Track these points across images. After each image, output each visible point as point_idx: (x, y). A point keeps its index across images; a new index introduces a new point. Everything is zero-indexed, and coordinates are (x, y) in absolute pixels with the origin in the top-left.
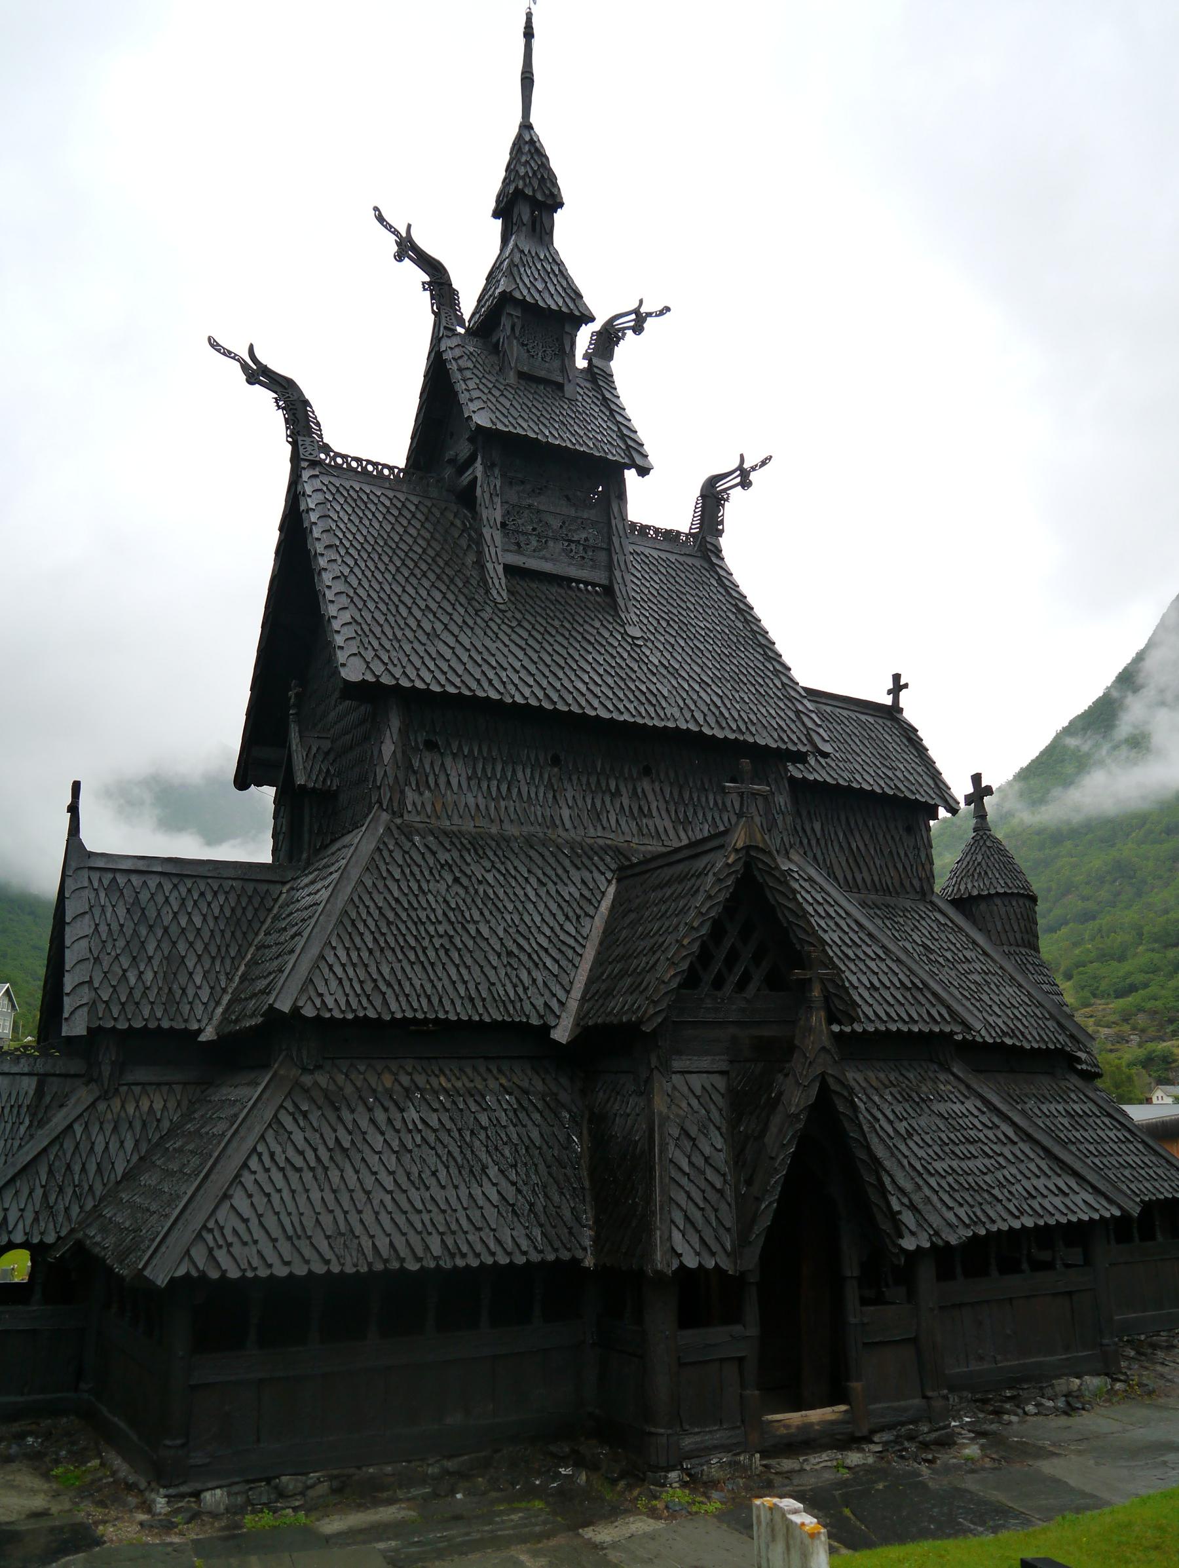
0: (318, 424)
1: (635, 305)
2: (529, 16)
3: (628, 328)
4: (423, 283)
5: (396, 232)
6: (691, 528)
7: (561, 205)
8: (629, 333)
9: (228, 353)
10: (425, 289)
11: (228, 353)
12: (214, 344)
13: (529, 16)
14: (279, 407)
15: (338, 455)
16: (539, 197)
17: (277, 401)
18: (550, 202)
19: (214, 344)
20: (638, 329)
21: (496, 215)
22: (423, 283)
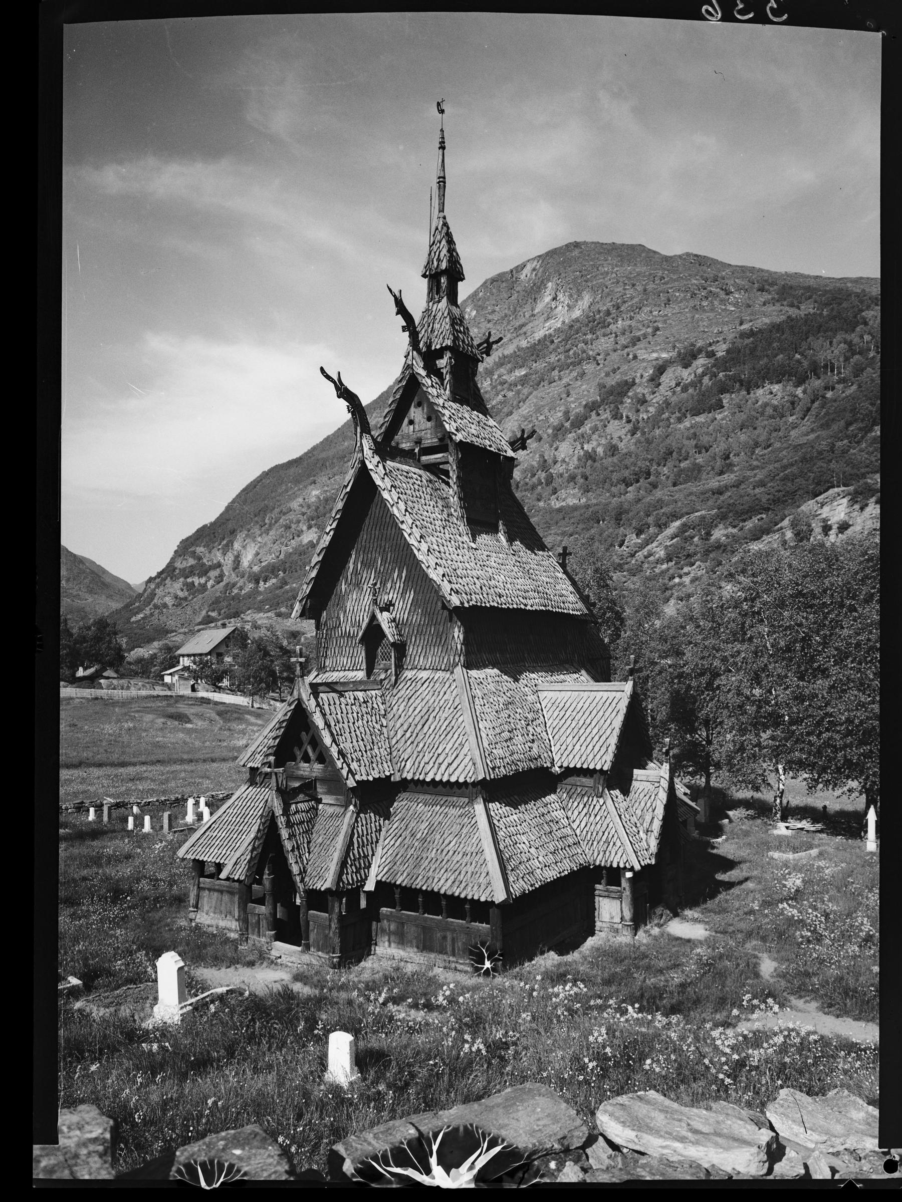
2: (442, 130)
4: (403, 327)
5: (395, 296)
7: (462, 279)
9: (328, 377)
10: (404, 331)
11: (328, 377)
13: (442, 130)
14: (349, 411)
21: (424, 276)
22: (403, 327)
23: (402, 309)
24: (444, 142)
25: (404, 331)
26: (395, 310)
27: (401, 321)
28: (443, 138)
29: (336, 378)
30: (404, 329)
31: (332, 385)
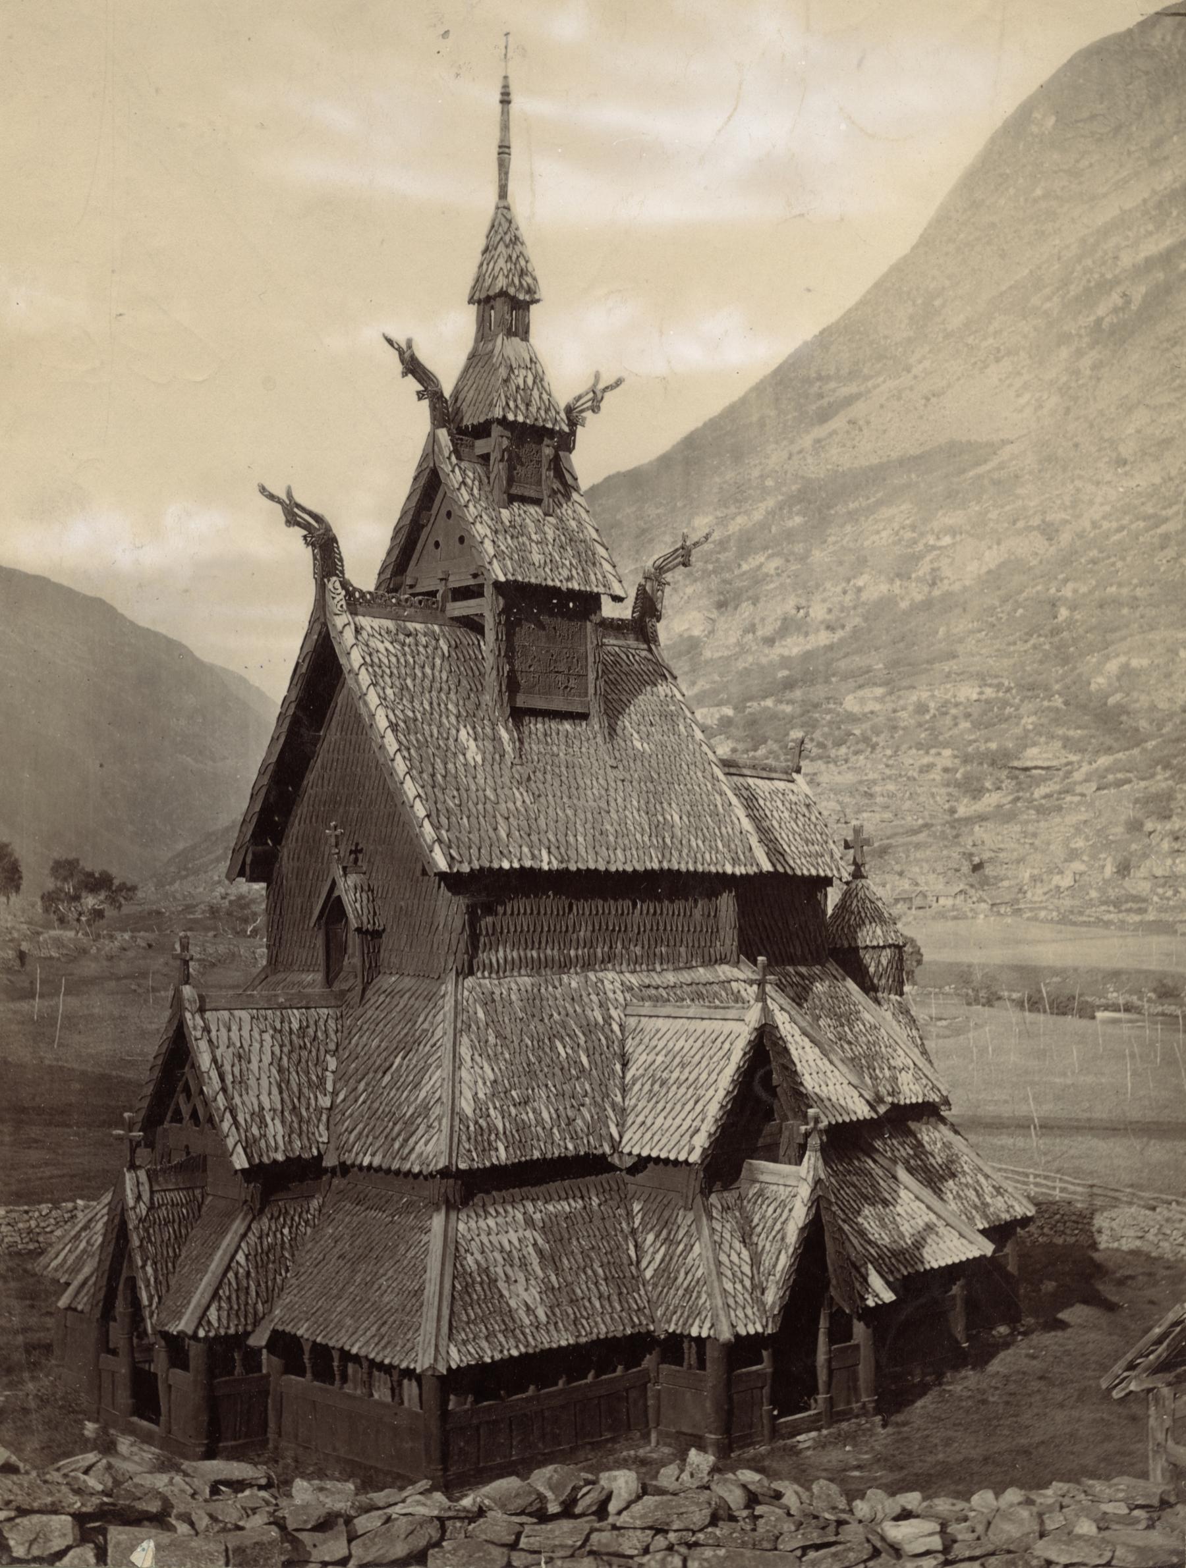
0: (341, 560)
1: (591, 382)
2: (506, 77)
3: (588, 409)
4: (418, 393)
6: (633, 612)
8: (588, 414)
9: (272, 497)
10: (420, 399)
11: (272, 497)
12: (263, 490)
13: (506, 77)
15: (355, 589)
16: (521, 297)
17: (305, 537)
18: (528, 298)
19: (263, 490)
20: (595, 409)
22: (418, 393)
23: (413, 366)
24: (508, 94)
25: (420, 399)
26: (399, 368)
27: (412, 385)
28: (506, 86)
29: (283, 496)
30: (420, 396)
31: (279, 507)
